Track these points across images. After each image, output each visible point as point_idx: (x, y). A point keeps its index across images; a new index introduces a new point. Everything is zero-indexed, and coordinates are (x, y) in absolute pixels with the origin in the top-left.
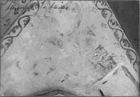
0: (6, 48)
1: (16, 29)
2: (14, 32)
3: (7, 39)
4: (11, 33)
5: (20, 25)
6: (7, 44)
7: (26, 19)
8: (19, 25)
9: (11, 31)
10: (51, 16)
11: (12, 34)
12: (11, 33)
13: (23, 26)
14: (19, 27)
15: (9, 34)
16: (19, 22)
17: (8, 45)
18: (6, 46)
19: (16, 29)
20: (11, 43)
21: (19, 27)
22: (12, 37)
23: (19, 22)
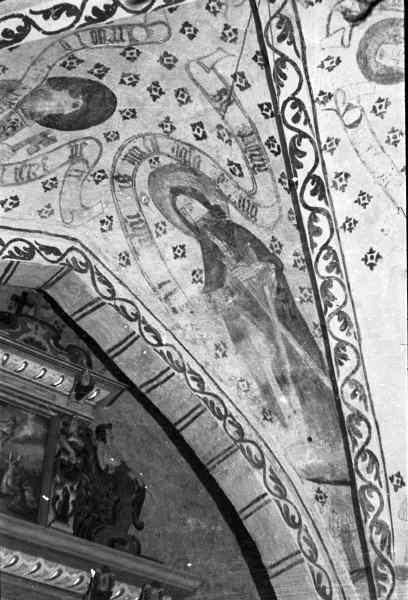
0: (339, 276)
1: (315, 224)
2: (318, 232)
3: (321, 259)
4: (315, 239)
5: (317, 208)
6: (328, 269)
7: (312, 187)
8: (314, 210)
9: (311, 238)
10: (362, 110)
11: (320, 241)
12: (315, 239)
13: (321, 204)
14: (318, 215)
15: (314, 245)
16: (306, 207)
17: (334, 266)
18: (333, 274)
19: (315, 224)
20: (336, 257)
21: (318, 215)
22: (325, 246)
23: (306, 207)
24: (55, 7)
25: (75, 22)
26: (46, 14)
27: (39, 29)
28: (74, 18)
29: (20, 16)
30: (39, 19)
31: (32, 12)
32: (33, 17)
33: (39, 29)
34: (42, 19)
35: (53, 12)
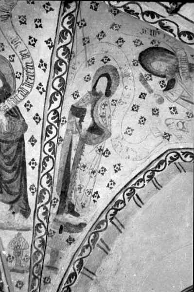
24: (166, 30)
25: (163, 20)
26: (171, 31)
27: (178, 30)
28: (163, 22)
29: (180, 39)
30: (175, 32)
31: (175, 36)
32: (176, 34)
33: (178, 30)
34: (174, 30)
35: (168, 30)
